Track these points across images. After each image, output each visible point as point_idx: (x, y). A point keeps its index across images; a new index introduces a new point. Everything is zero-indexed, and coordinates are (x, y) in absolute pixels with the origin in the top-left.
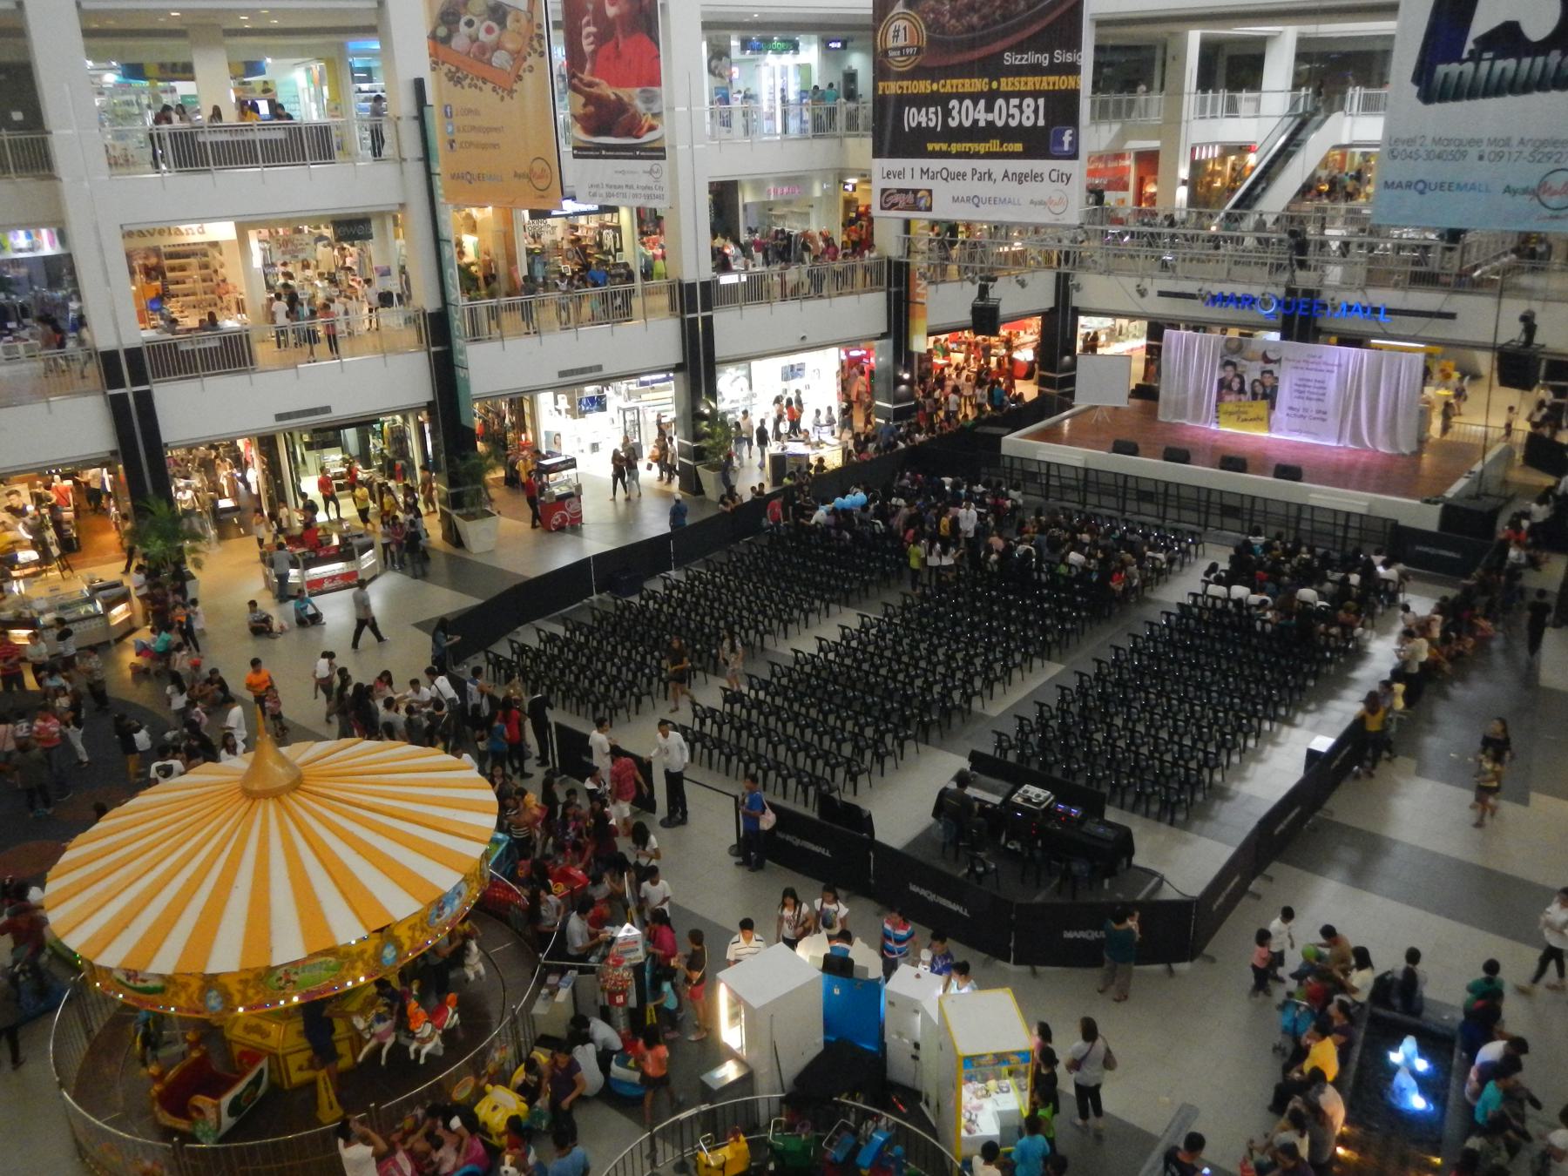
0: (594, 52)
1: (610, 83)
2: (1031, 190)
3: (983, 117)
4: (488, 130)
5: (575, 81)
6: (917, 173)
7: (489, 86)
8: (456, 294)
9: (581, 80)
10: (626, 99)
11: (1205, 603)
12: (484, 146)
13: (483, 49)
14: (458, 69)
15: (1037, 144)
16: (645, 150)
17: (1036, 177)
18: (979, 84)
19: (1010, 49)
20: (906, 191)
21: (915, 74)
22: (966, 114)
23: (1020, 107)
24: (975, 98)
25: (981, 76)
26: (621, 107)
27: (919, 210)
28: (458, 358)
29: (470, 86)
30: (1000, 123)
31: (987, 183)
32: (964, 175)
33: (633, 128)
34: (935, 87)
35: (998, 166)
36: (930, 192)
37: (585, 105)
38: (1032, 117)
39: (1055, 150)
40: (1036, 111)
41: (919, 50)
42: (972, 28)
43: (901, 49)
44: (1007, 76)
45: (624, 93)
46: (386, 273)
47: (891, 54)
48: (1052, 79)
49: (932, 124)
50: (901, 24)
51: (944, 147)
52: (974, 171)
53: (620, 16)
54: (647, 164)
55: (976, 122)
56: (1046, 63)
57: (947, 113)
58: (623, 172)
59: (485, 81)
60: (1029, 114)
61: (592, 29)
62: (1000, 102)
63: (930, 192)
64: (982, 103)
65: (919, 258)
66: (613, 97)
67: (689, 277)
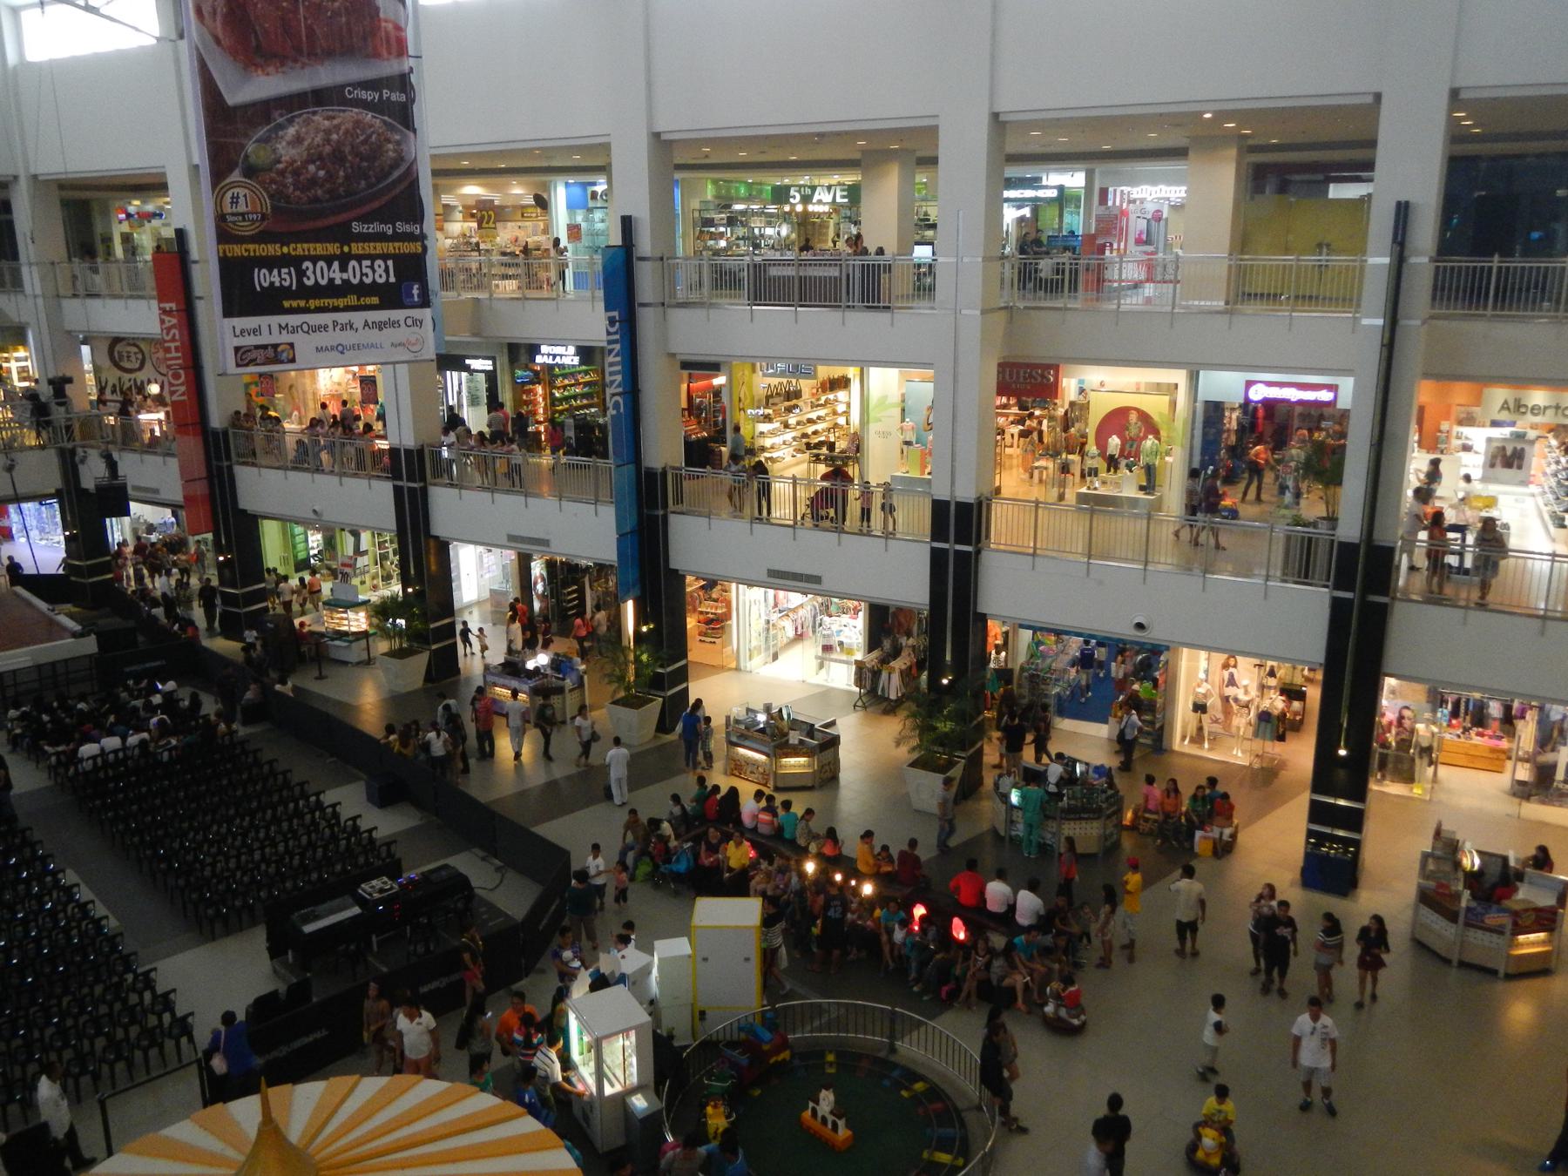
2: (389, 334)
3: (338, 277)
6: (275, 329)
11: (105, 762)
15: (391, 297)
17: (394, 324)
18: (333, 248)
19: (358, 219)
20: (265, 347)
21: (262, 238)
22: (317, 274)
23: (372, 267)
24: (329, 261)
25: (334, 241)
27: (282, 362)
30: (355, 281)
31: (349, 333)
32: (326, 327)
34: (285, 250)
35: (358, 318)
36: (292, 345)
38: (384, 275)
39: (407, 301)
40: (387, 270)
41: (264, 217)
42: (316, 200)
43: (243, 214)
44: (357, 242)
47: (230, 218)
48: (397, 244)
49: (286, 284)
50: (242, 192)
51: (302, 303)
52: (335, 323)
55: (331, 280)
56: (390, 232)
57: (301, 274)
60: (381, 273)
62: (353, 263)
63: (292, 345)
64: (336, 265)
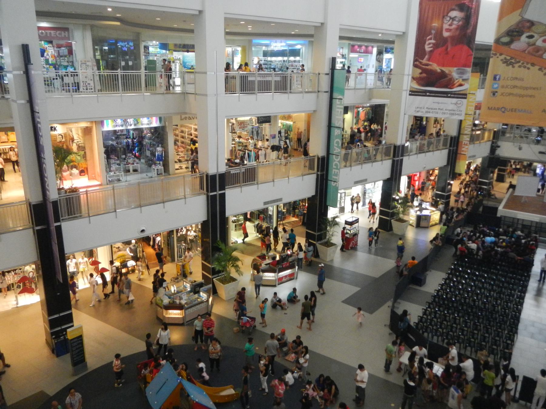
0: (431, 51)
1: (439, 65)
4: (527, 88)
5: (417, 63)
7: (537, 67)
8: (336, 149)
9: (421, 63)
10: (447, 72)
12: (522, 96)
13: (538, 49)
14: (512, 58)
16: (455, 94)
26: (443, 75)
28: (331, 176)
29: (520, 67)
33: (450, 83)
37: (421, 73)
45: (446, 70)
46: (274, 137)
53: (452, 38)
54: (454, 100)
58: (438, 103)
59: (533, 65)
61: (433, 41)
65: (465, 137)
66: (439, 71)
67: (399, 143)
